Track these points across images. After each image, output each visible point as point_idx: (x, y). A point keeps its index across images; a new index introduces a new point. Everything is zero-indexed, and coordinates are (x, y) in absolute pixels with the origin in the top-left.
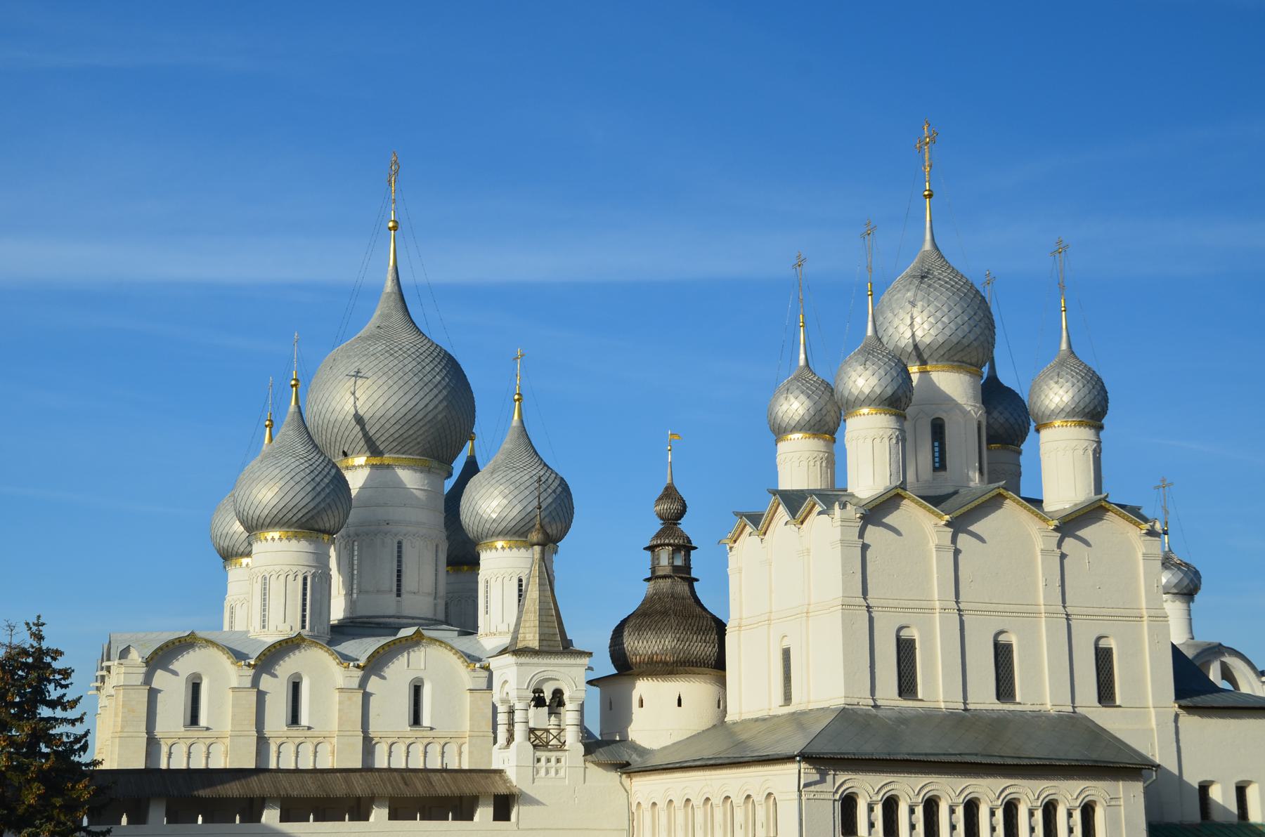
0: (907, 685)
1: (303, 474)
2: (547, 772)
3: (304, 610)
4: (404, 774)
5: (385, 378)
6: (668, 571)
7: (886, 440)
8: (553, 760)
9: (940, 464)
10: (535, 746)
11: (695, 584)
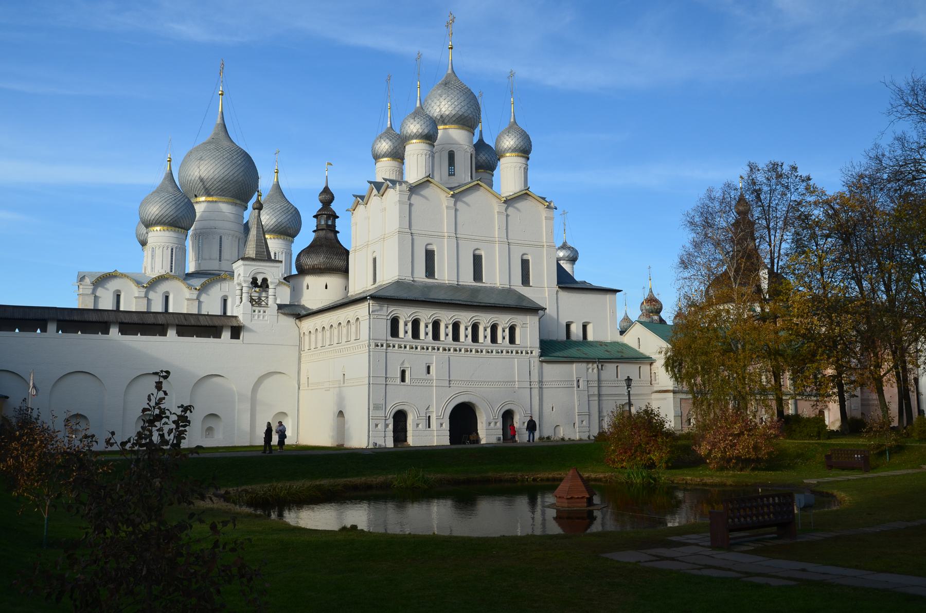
0: (430, 271)
1: (171, 200)
2: (258, 317)
3: (172, 263)
4: (186, 316)
5: (214, 160)
6: (324, 227)
7: (424, 156)
8: (262, 311)
9: (452, 174)
10: (252, 305)
11: (338, 235)
